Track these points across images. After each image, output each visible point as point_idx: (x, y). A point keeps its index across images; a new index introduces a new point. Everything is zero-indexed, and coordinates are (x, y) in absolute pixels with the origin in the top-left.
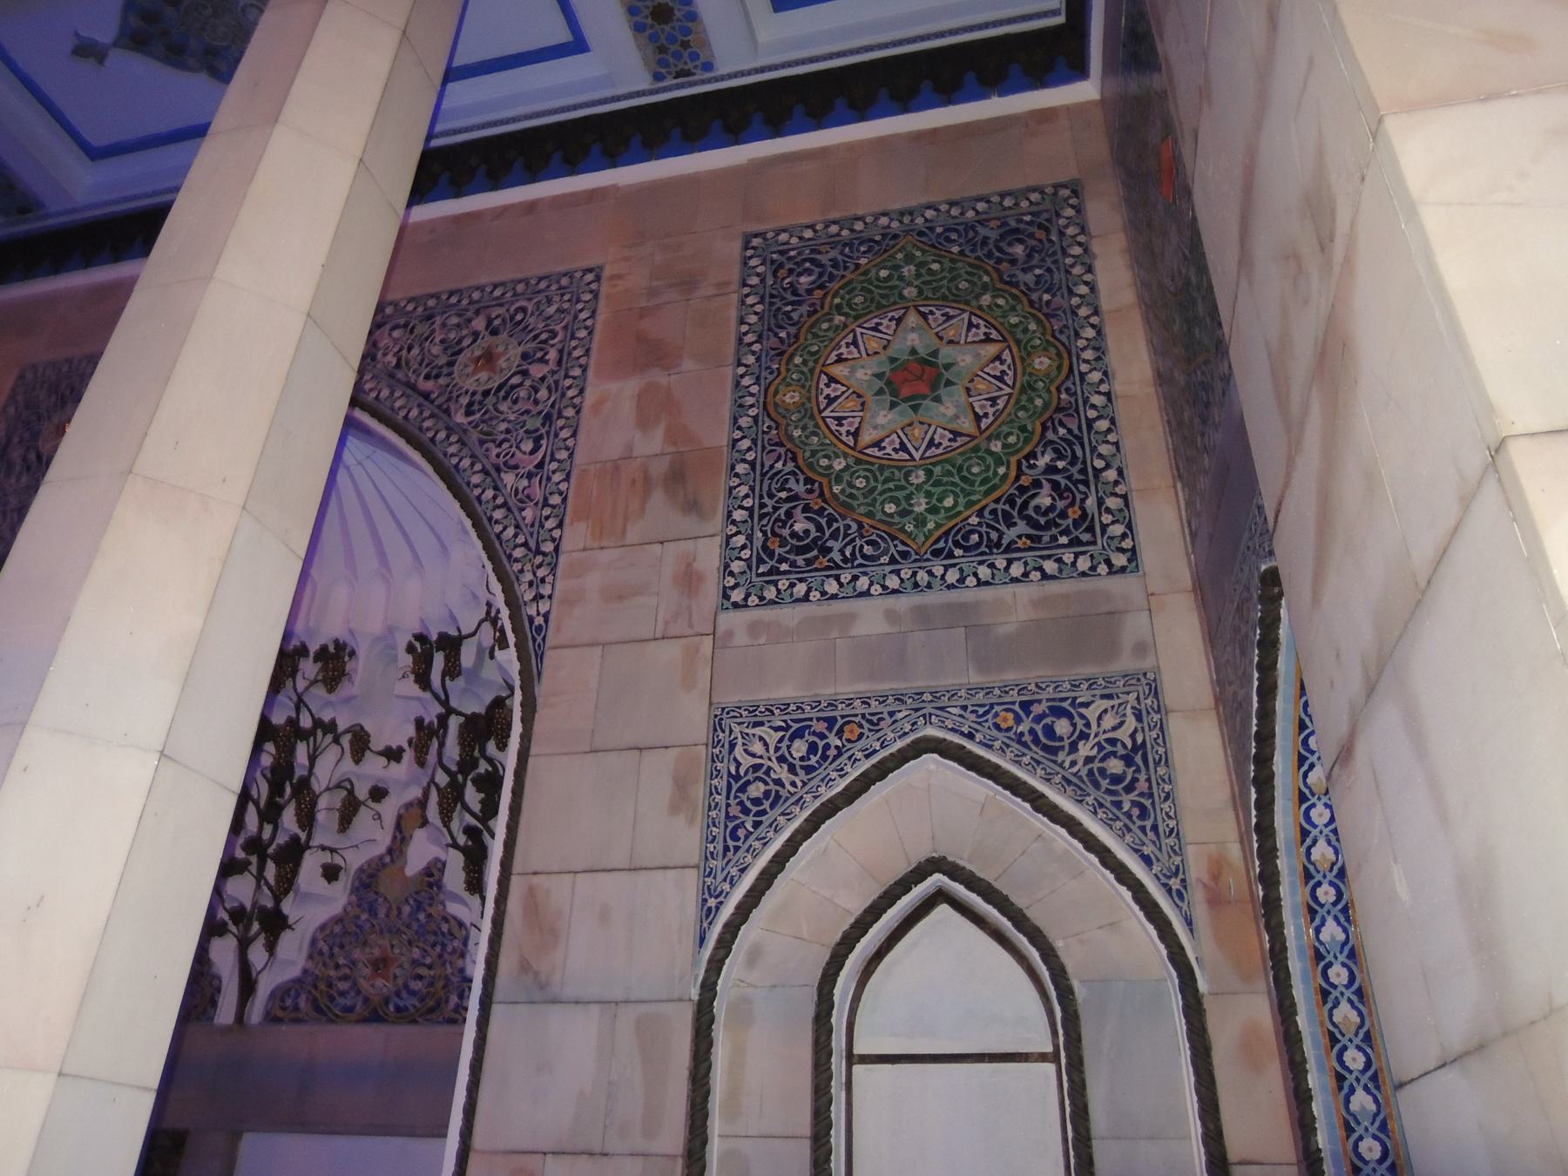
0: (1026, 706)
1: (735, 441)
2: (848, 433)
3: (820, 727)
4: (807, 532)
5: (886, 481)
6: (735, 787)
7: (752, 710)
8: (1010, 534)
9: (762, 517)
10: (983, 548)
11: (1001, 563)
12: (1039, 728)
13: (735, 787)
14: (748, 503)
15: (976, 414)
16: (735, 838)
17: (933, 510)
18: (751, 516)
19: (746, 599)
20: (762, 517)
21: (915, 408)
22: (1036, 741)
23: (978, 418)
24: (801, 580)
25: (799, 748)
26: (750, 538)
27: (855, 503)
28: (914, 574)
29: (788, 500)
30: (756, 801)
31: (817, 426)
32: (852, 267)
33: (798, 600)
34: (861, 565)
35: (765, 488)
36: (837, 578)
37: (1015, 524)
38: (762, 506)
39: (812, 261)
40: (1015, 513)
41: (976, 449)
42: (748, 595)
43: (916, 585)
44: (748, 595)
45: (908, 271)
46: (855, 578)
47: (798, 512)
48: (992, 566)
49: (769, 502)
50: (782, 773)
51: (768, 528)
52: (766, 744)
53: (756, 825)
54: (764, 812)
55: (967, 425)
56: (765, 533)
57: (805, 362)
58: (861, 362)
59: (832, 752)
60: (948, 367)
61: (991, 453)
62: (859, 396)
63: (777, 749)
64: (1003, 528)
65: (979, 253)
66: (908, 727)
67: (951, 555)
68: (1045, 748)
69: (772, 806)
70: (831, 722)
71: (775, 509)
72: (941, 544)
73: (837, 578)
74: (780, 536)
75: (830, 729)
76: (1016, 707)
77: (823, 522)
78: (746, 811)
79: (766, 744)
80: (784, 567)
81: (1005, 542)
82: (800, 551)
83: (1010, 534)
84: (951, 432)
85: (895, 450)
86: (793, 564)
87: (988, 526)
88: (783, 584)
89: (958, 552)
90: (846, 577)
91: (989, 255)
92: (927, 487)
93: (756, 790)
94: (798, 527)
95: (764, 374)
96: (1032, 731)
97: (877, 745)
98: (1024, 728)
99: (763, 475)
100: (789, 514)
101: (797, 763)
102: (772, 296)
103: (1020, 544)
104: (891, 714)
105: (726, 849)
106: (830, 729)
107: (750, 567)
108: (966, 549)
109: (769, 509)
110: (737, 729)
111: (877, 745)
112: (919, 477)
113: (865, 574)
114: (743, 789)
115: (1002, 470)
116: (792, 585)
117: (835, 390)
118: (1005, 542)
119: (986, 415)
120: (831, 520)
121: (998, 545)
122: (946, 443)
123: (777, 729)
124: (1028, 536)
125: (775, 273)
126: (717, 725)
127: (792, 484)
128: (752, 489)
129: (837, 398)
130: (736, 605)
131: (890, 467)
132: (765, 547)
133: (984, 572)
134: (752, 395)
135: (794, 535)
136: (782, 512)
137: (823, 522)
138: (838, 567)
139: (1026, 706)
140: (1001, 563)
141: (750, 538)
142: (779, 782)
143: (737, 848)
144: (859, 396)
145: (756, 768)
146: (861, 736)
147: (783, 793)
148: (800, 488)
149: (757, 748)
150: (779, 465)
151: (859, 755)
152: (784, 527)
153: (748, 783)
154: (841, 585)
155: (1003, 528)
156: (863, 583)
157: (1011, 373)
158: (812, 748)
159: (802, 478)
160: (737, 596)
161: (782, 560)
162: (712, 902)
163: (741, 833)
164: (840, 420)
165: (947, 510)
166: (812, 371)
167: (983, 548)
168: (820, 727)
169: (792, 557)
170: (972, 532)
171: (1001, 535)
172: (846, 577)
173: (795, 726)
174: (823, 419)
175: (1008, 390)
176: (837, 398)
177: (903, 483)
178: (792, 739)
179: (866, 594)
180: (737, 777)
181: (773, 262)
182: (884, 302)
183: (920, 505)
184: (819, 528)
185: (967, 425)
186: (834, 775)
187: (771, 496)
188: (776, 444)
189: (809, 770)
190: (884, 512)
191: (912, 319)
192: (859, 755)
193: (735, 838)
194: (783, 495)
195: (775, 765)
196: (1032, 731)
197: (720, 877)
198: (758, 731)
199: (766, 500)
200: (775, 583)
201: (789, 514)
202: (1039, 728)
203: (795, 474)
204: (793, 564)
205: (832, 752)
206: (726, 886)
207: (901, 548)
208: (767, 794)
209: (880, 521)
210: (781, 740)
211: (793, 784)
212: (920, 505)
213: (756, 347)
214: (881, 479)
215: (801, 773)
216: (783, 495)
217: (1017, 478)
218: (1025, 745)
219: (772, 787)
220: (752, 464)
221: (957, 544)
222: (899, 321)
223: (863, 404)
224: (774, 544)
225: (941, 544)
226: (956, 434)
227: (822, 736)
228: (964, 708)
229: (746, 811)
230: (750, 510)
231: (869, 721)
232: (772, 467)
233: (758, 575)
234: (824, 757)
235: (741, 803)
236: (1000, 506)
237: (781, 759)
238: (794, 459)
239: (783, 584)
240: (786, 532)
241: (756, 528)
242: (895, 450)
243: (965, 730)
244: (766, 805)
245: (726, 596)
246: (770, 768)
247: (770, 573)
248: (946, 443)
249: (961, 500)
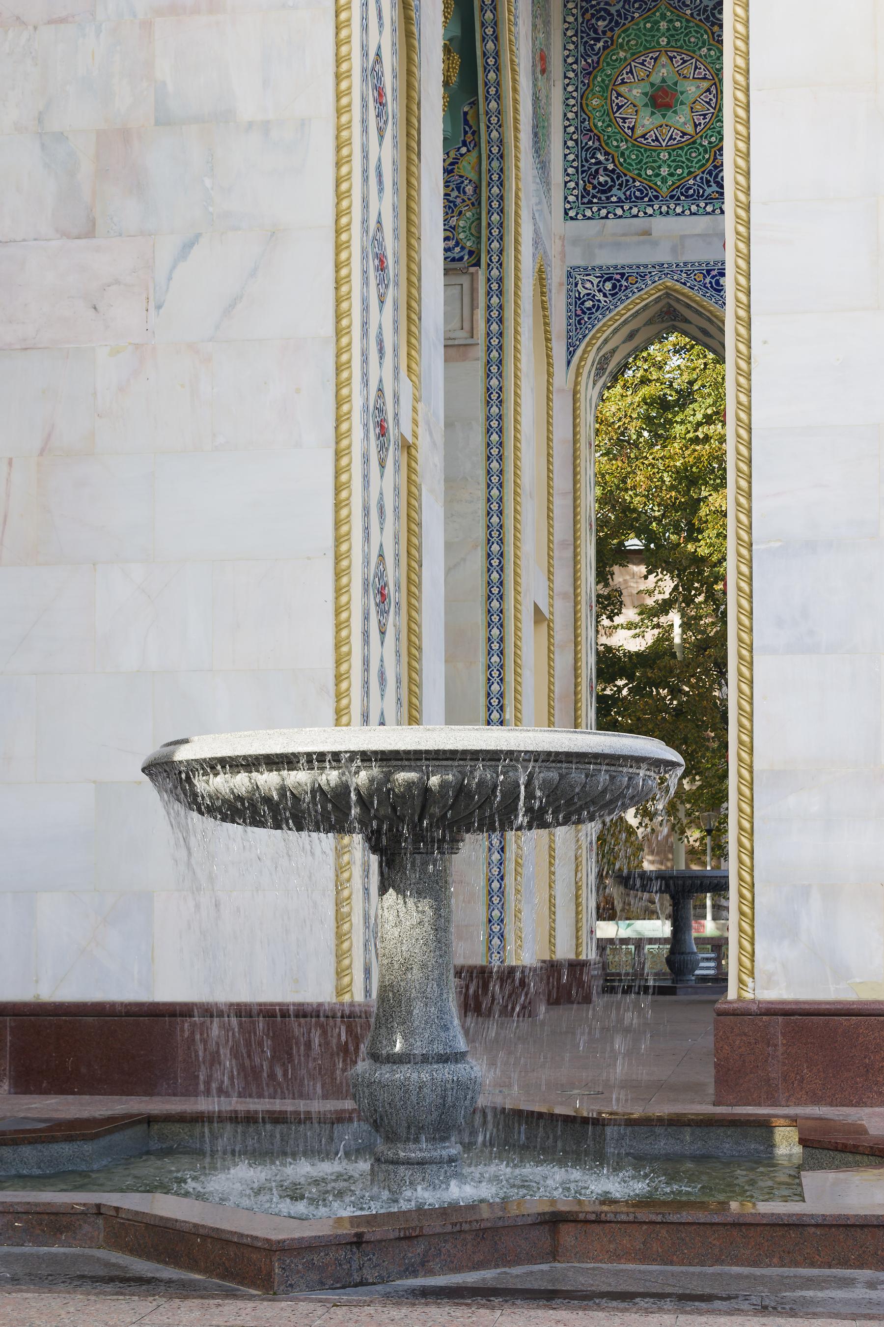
0: (709, 272)
1: (566, 127)
2: (629, 127)
3: (618, 277)
4: (606, 182)
5: (647, 157)
6: (579, 302)
7: (586, 269)
8: (709, 191)
9: (583, 172)
10: (695, 197)
11: (702, 205)
12: (713, 281)
13: (579, 302)
14: (575, 164)
15: (695, 123)
16: (580, 323)
17: (671, 175)
18: (577, 172)
19: (576, 215)
20: (583, 172)
21: (664, 116)
22: (712, 287)
23: (696, 126)
24: (603, 208)
25: (608, 286)
26: (577, 184)
27: (631, 168)
28: (660, 207)
29: (595, 164)
30: (589, 309)
31: (610, 121)
32: (630, 19)
33: (602, 218)
34: (634, 202)
35: (584, 156)
36: (622, 207)
37: (711, 186)
38: (583, 166)
39: (605, 10)
40: (712, 180)
41: (694, 142)
42: (577, 214)
43: (661, 213)
44: (577, 214)
45: (663, 25)
46: (631, 208)
47: (601, 171)
48: (698, 206)
49: (587, 165)
50: (600, 296)
51: (586, 179)
52: (592, 283)
53: (589, 318)
54: (593, 313)
55: (690, 129)
56: (584, 182)
57: (603, 81)
58: (634, 85)
59: (623, 288)
60: (682, 93)
61: (702, 146)
62: (635, 106)
63: (598, 286)
64: (706, 187)
65: (702, 17)
66: (657, 279)
67: (679, 199)
68: (716, 290)
69: (597, 311)
70: (622, 275)
71: (589, 168)
72: (674, 193)
73: (622, 207)
74: (592, 184)
75: (622, 278)
76: (704, 272)
77: (615, 177)
78: (584, 313)
79: (592, 283)
80: (595, 200)
81: (706, 194)
82: (603, 192)
83: (709, 191)
84: (682, 132)
85: (653, 140)
86: (600, 199)
87: (698, 186)
88: (595, 209)
89: (683, 198)
90: (626, 207)
91: (707, 19)
92: (668, 162)
93: (589, 304)
94: (602, 179)
95: (580, 86)
96: (711, 283)
97: (643, 286)
98: (708, 280)
99: (582, 148)
100: (597, 171)
101: (607, 293)
102: (582, 32)
103: (713, 196)
104: (650, 273)
105: (576, 329)
106: (622, 278)
107: (577, 199)
108: (687, 197)
109: (586, 168)
110: (578, 277)
111: (643, 286)
112: (664, 155)
113: (636, 206)
114: (583, 303)
115: (707, 156)
116: (599, 210)
117: (622, 101)
118: (706, 194)
119: (700, 124)
120: (618, 178)
121: (702, 196)
122: (678, 138)
123: (597, 277)
124: (717, 192)
125: (583, 15)
126: (569, 275)
127: (599, 156)
128: (577, 156)
129: (623, 106)
130: (572, 218)
131: (650, 150)
132: (585, 189)
133: (694, 208)
134: (574, 98)
135: (600, 183)
136: (593, 170)
137: (615, 177)
138: (623, 202)
139: (709, 272)
140: (702, 205)
141: (577, 184)
142: (599, 301)
143: (581, 328)
144: (635, 106)
145: (588, 294)
146: (637, 282)
147: (601, 305)
148: (601, 158)
149: (588, 285)
150: (590, 143)
151: (636, 290)
152: (594, 179)
153: (585, 301)
154: (624, 211)
155: (706, 187)
156: (635, 211)
157: (714, 100)
158: (614, 287)
159: (603, 151)
160: (572, 213)
161: (594, 196)
162: (571, 349)
163: (583, 322)
164: (624, 119)
165: (679, 175)
166: (607, 86)
167: (695, 197)
168: (618, 277)
169: (599, 195)
170: (690, 188)
171: (704, 191)
172: (626, 207)
173: (606, 276)
174: (615, 118)
175: (712, 111)
176: (623, 106)
177: (656, 158)
178: (604, 282)
179: (636, 216)
180: (579, 299)
181: (582, 7)
182: (648, 45)
183: (664, 171)
184: (613, 180)
185: (690, 129)
186: (624, 298)
187: (587, 161)
188: (588, 130)
189: (613, 295)
190: (646, 174)
191: (664, 59)
192: (636, 290)
193: (580, 323)
194: (593, 161)
195: (597, 294)
196: (711, 283)
197: (574, 339)
198: (588, 278)
199: (584, 163)
200: (591, 208)
201: (597, 171)
202: (713, 281)
203: (599, 150)
204: (600, 199)
205: (623, 288)
206: (578, 343)
207: (655, 193)
208: (594, 306)
209: (645, 179)
210: (599, 282)
211: (605, 302)
212: (664, 171)
213: (575, 66)
214: (645, 156)
215: (610, 297)
216: (593, 161)
217: (713, 162)
218: (707, 288)
219: (597, 303)
220: (576, 141)
221: (682, 194)
222: (656, 59)
223: (636, 111)
224: (589, 187)
225: (674, 193)
226: (684, 134)
227: (619, 281)
228: (682, 271)
229: (584, 313)
230: (576, 168)
231: (641, 276)
232: (586, 144)
233: (582, 204)
234: (620, 290)
235: (582, 310)
236: (705, 176)
237: (600, 291)
238: (599, 140)
239: (595, 209)
240: (595, 182)
241: (580, 178)
242: (653, 140)
243: (683, 281)
244: (594, 310)
245: (566, 213)
246: (594, 295)
247: (588, 203)
248: (678, 138)
249: (686, 171)
